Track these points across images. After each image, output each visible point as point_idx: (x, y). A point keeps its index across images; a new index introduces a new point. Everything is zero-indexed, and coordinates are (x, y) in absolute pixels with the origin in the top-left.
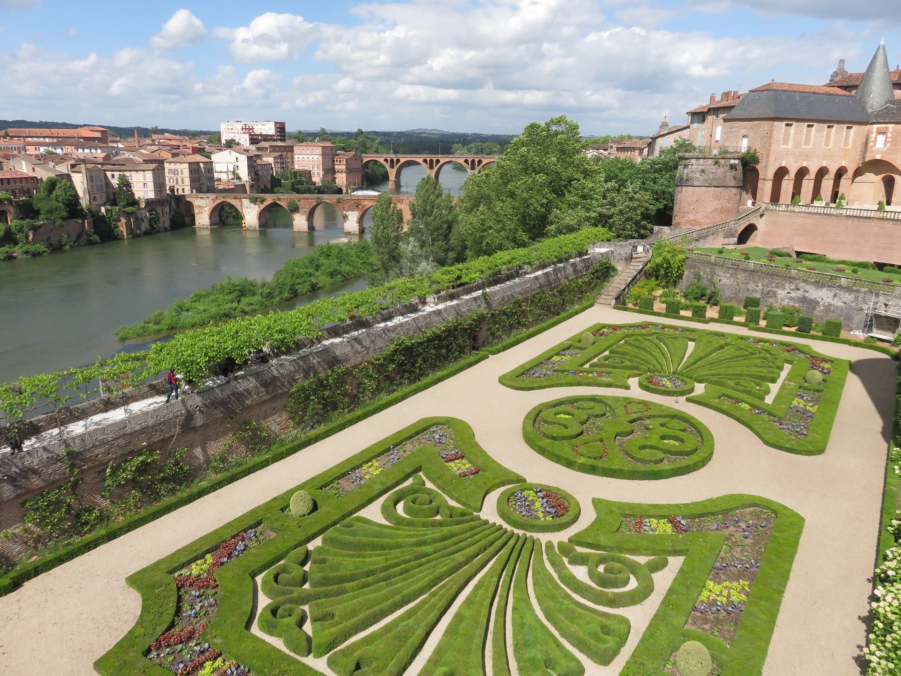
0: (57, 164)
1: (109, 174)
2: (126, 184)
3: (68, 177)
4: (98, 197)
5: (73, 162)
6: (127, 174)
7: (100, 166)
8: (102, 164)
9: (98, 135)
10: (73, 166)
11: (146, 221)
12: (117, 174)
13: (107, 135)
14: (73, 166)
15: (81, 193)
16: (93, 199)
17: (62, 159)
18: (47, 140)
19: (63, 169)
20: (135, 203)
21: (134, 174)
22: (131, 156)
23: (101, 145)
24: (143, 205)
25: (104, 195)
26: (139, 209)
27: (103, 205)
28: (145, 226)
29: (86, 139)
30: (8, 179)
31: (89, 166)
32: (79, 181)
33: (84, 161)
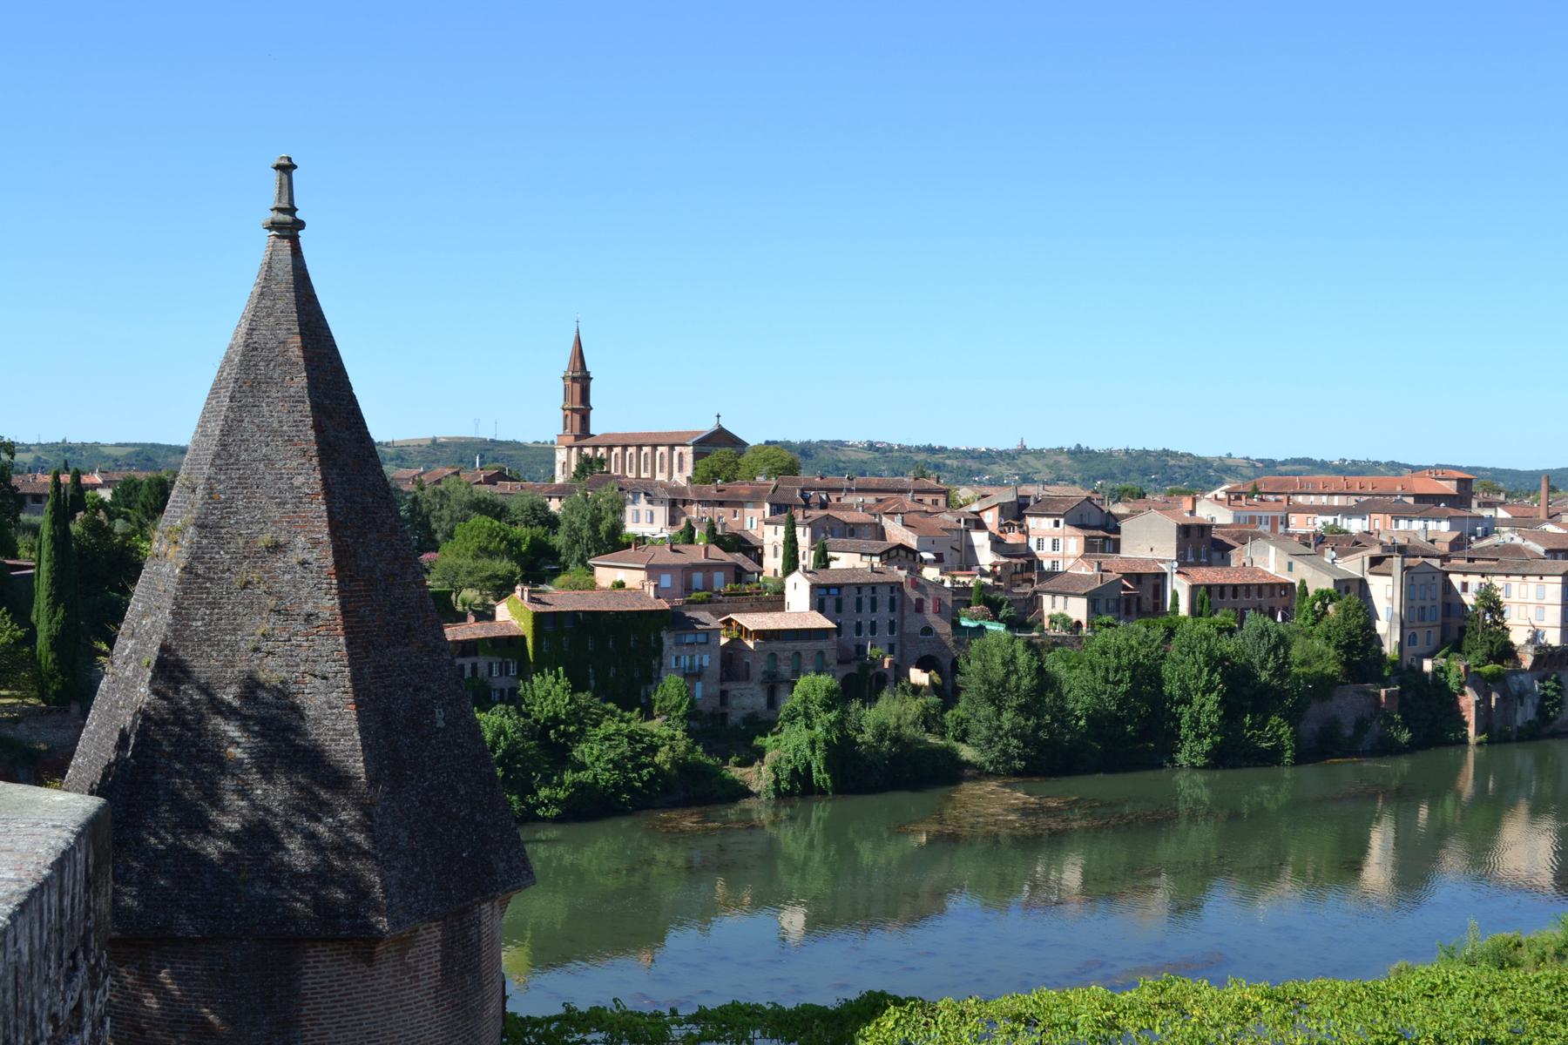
0: (1342, 554)
1: (1457, 580)
2: (1493, 606)
3: (1363, 583)
4: (1421, 635)
5: (1376, 551)
6: (1499, 581)
7: (1436, 563)
8: (1445, 558)
9: (1450, 487)
10: (1375, 561)
11: (1528, 701)
12: (1474, 581)
13: (1463, 493)
14: (1375, 561)
15: (1381, 627)
16: (1407, 639)
17: (1356, 543)
18: (1336, 501)
19: (1353, 566)
20: (1507, 652)
21: (1515, 581)
22: (1518, 540)
23: (1452, 512)
24: (1527, 662)
25: (1436, 633)
26: (1519, 671)
27: (1431, 656)
28: (1525, 714)
29: (1420, 498)
30: (1235, 587)
31: (1409, 561)
32: (1385, 593)
33: (1402, 550)
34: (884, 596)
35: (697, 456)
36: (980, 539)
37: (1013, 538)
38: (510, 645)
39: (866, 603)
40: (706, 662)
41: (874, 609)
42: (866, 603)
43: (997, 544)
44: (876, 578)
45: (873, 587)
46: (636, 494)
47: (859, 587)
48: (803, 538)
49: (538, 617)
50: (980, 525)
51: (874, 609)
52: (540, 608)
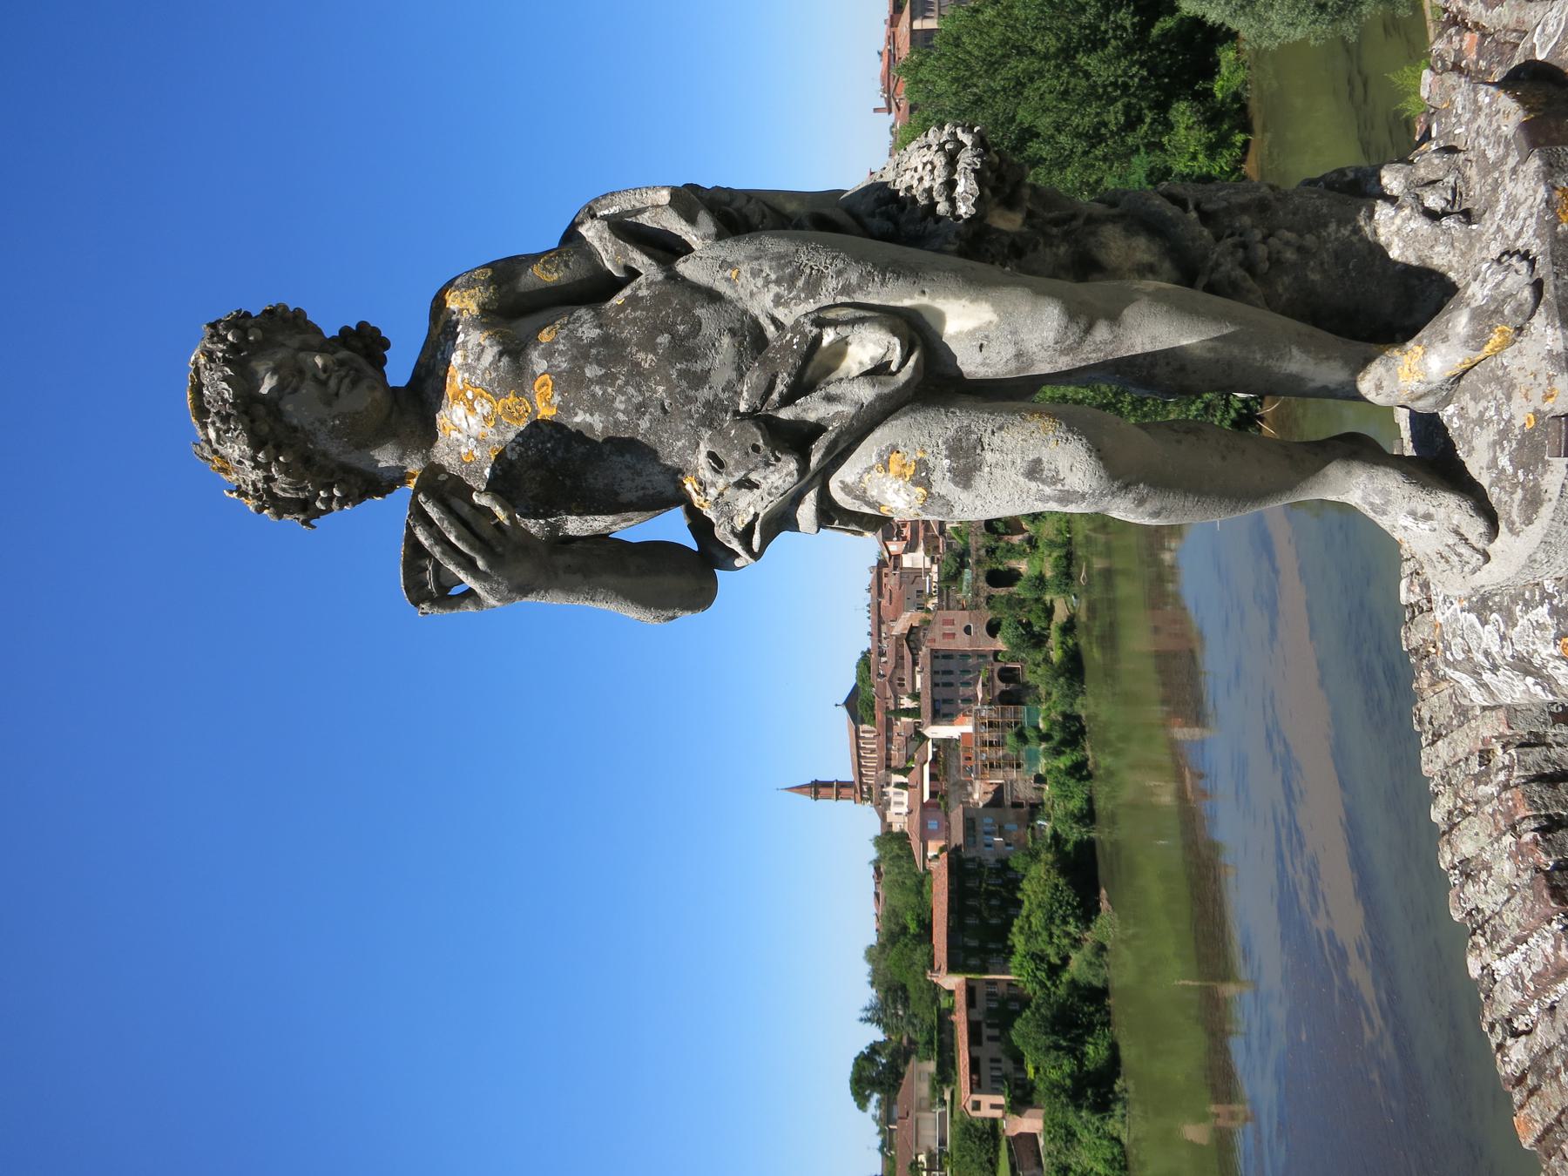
34: (942, 664)
35: (863, 722)
36: (907, 561)
37: (907, 532)
38: (971, 991)
39: (946, 678)
40: (990, 821)
41: (950, 672)
42: (946, 678)
43: (911, 548)
44: (928, 669)
45: (934, 673)
46: (884, 794)
47: (935, 685)
48: (907, 703)
49: (953, 968)
50: (897, 557)
51: (950, 672)
52: (944, 967)
